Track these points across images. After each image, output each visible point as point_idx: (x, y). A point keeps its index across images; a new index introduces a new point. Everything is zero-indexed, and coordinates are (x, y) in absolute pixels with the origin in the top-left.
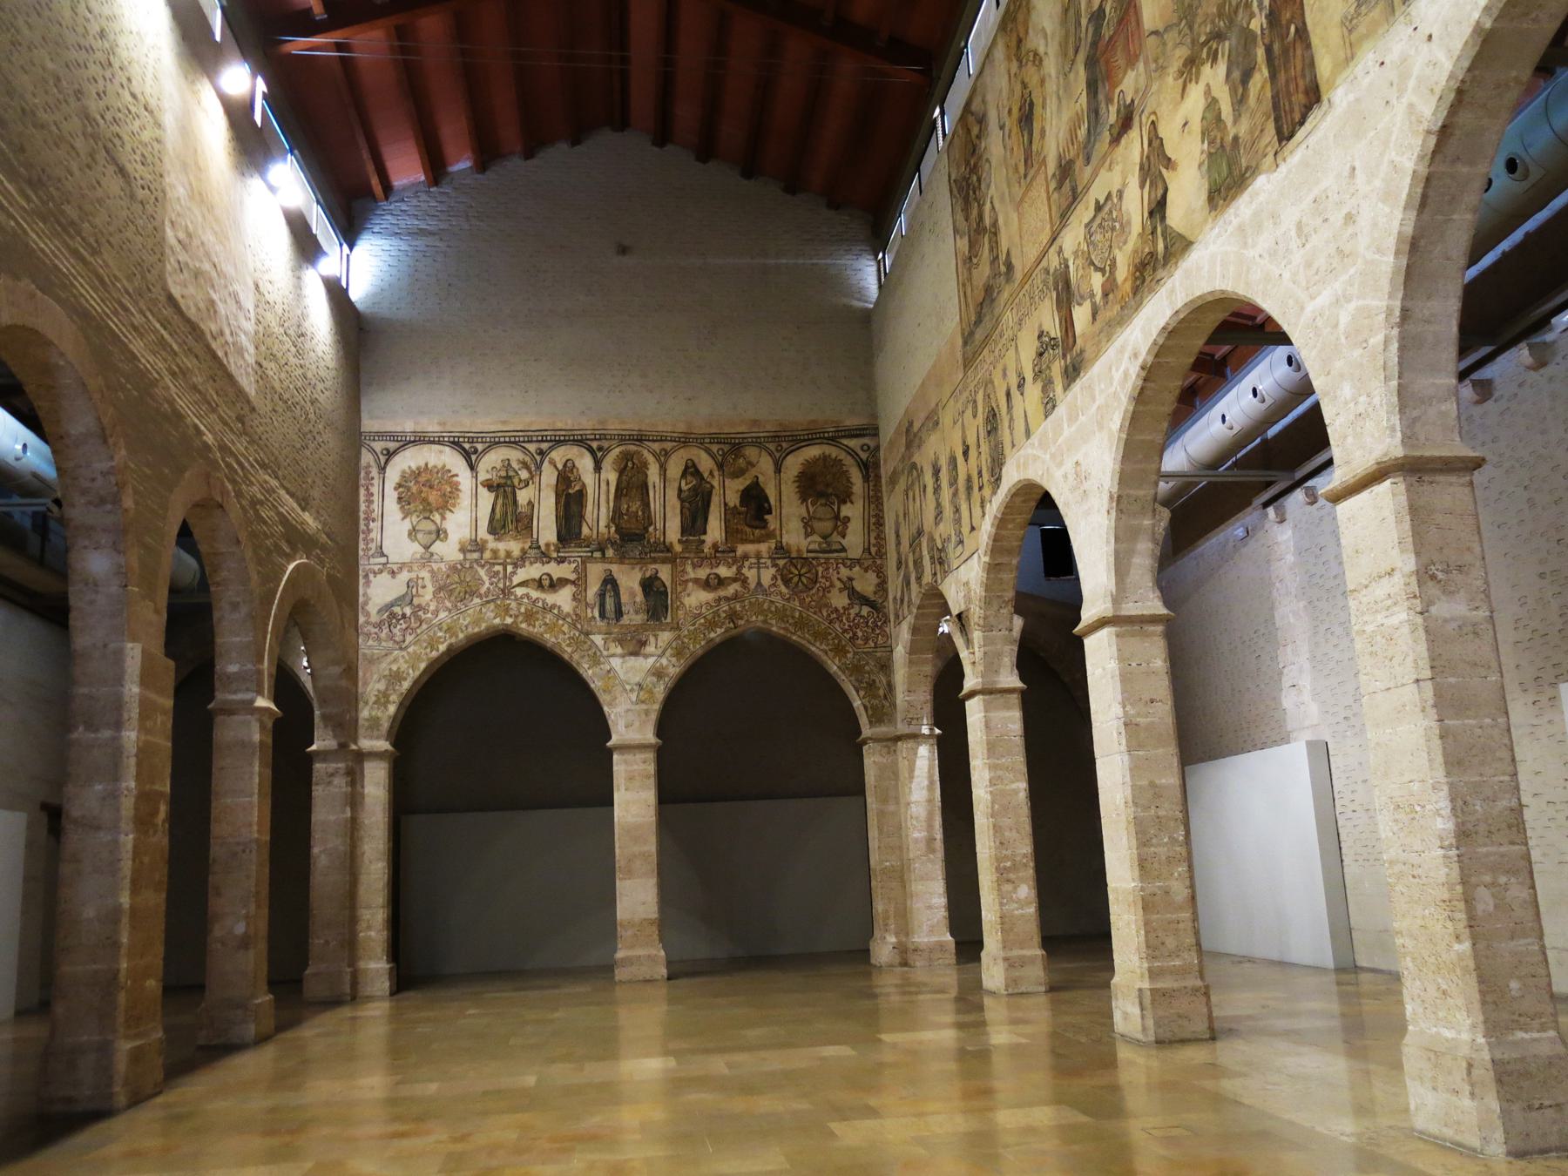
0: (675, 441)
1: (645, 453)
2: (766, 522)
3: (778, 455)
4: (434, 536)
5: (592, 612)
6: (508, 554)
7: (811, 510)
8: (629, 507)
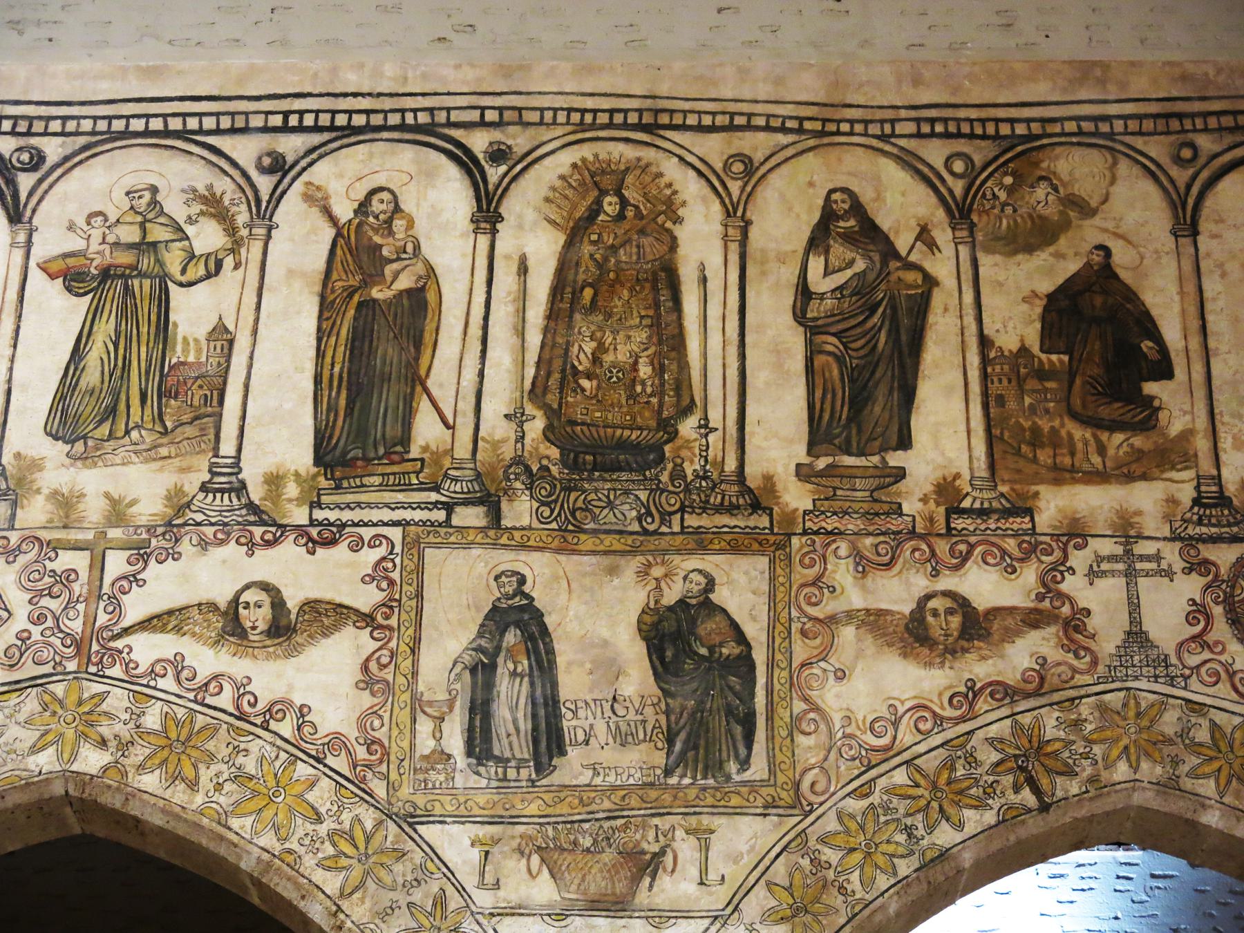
0: (783, 129)
1: (671, 169)
2: (1150, 408)
3: (1181, 176)
5: (437, 734)
6: (117, 511)
8: (601, 348)
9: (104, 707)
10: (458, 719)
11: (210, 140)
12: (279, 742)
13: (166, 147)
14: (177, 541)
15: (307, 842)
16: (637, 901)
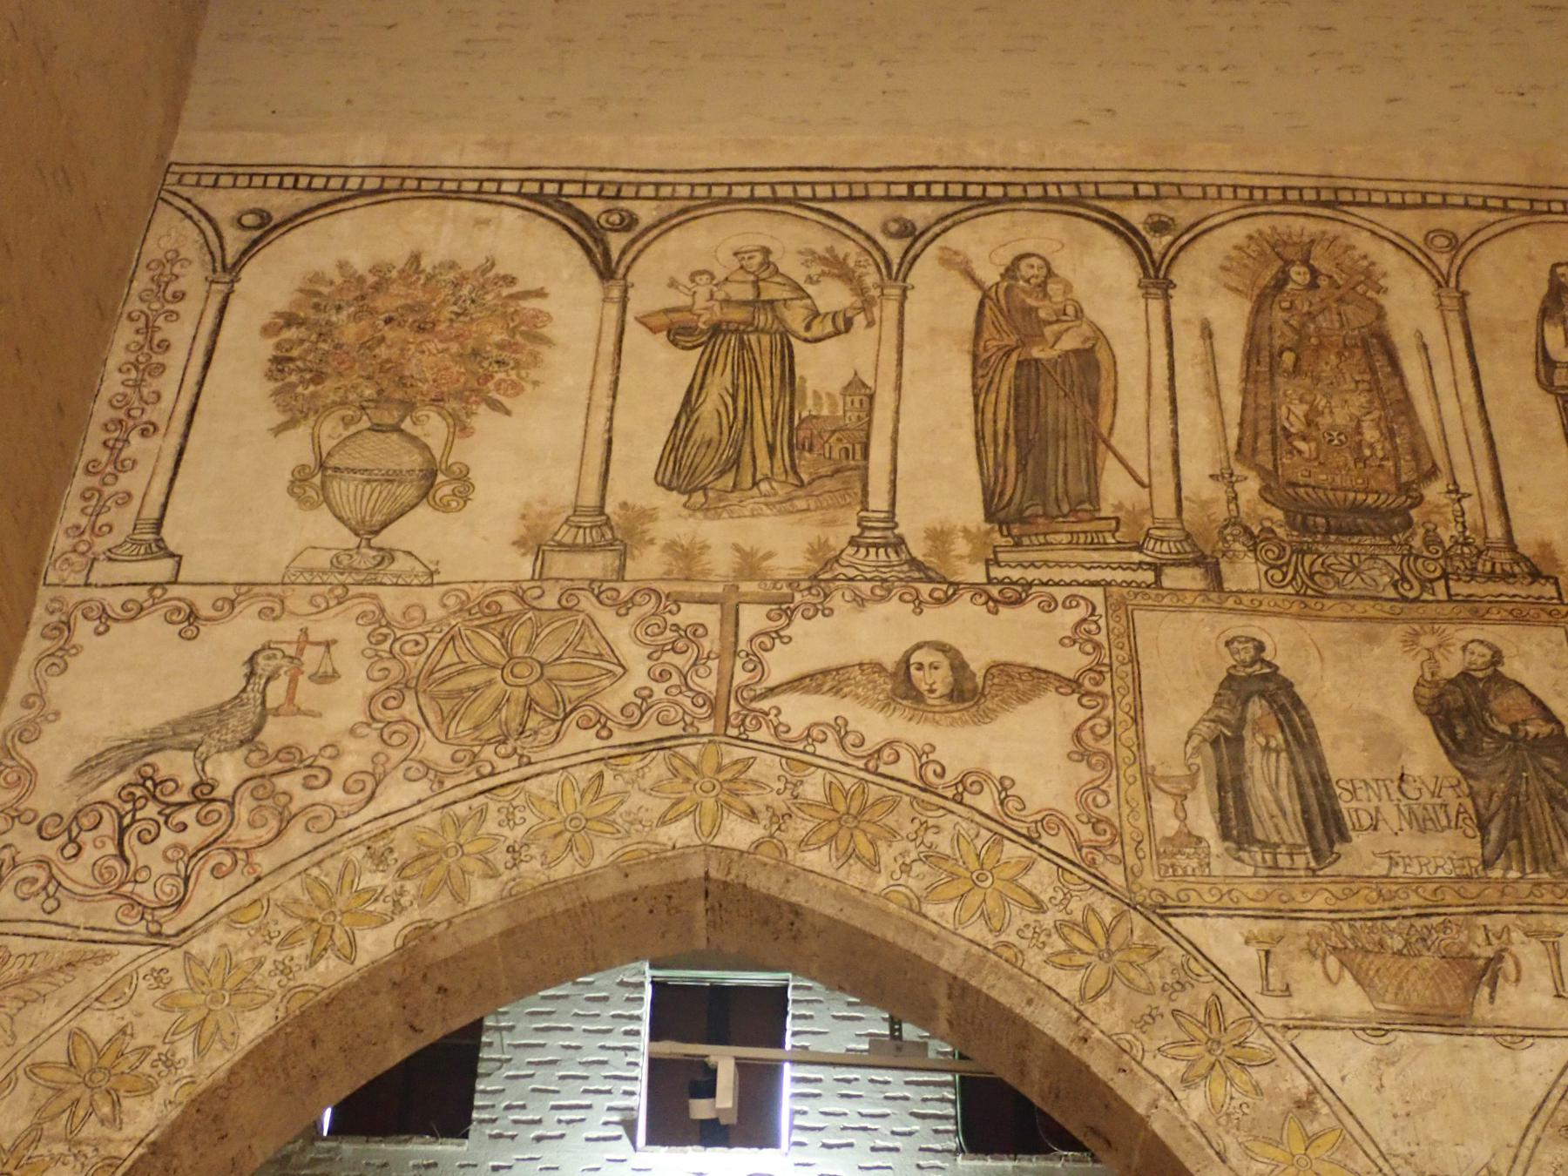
0: (1485, 207)
1: (1364, 243)
4: (408, 492)
6: (750, 564)
9: (751, 773)
10: (1204, 797)
11: (827, 207)
12: (978, 818)
13: (776, 212)
14: (826, 596)
15: (1029, 933)
16: (1477, 1014)
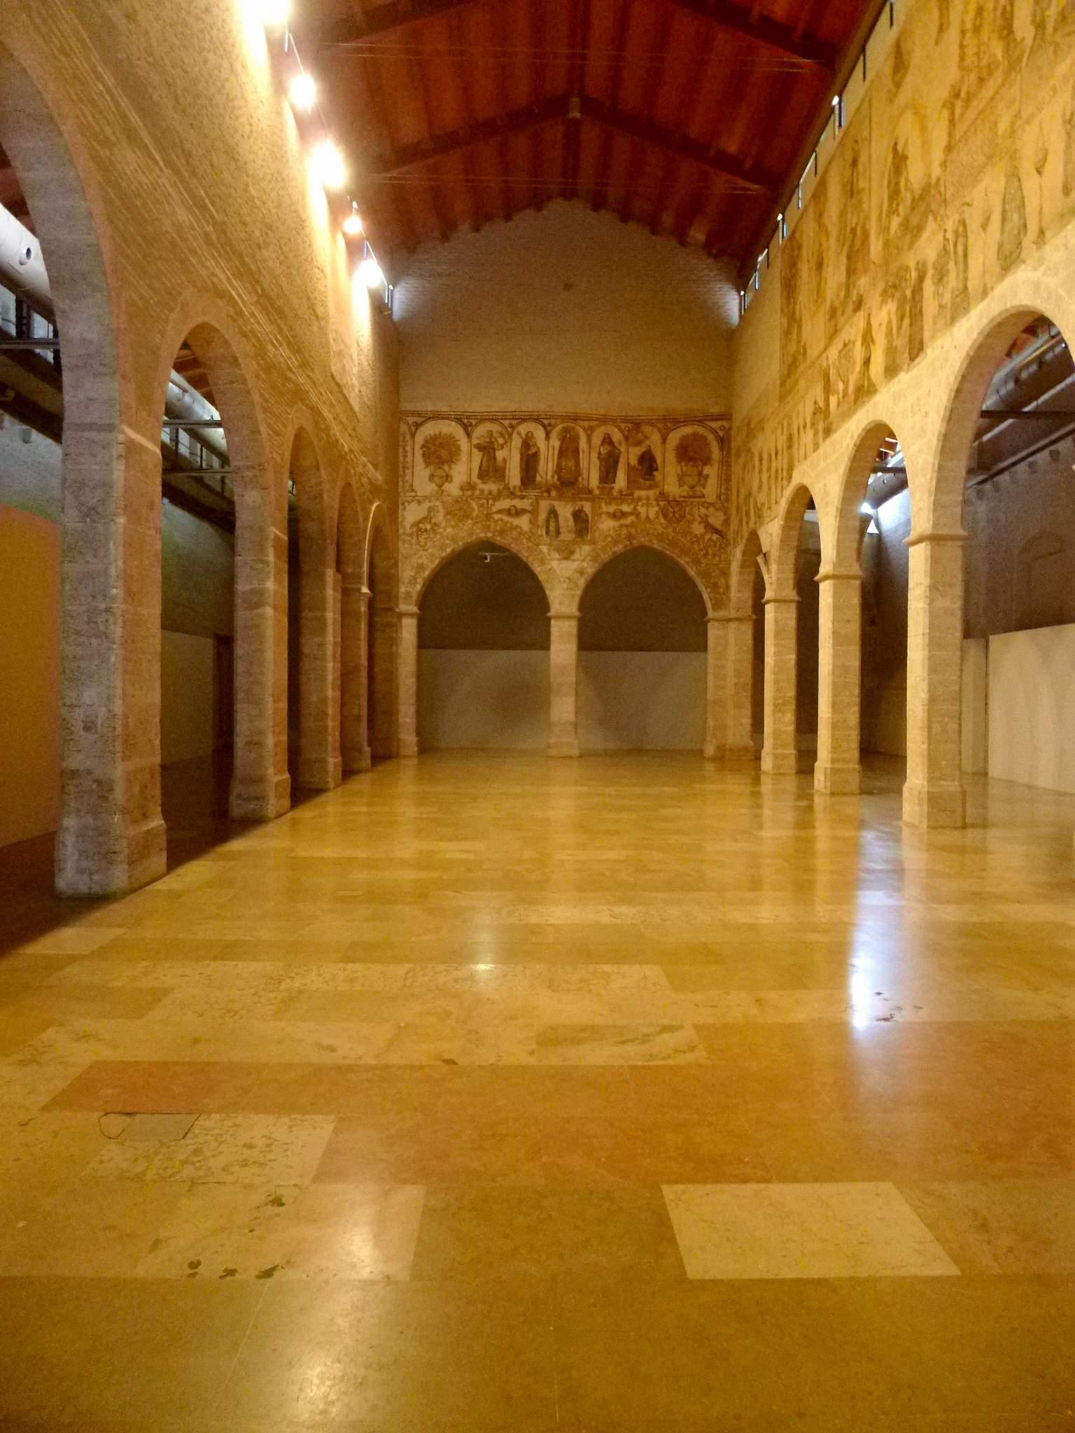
1: (578, 428)
2: (654, 476)
3: (664, 431)
4: (445, 479)
6: (490, 493)
7: (684, 469)
